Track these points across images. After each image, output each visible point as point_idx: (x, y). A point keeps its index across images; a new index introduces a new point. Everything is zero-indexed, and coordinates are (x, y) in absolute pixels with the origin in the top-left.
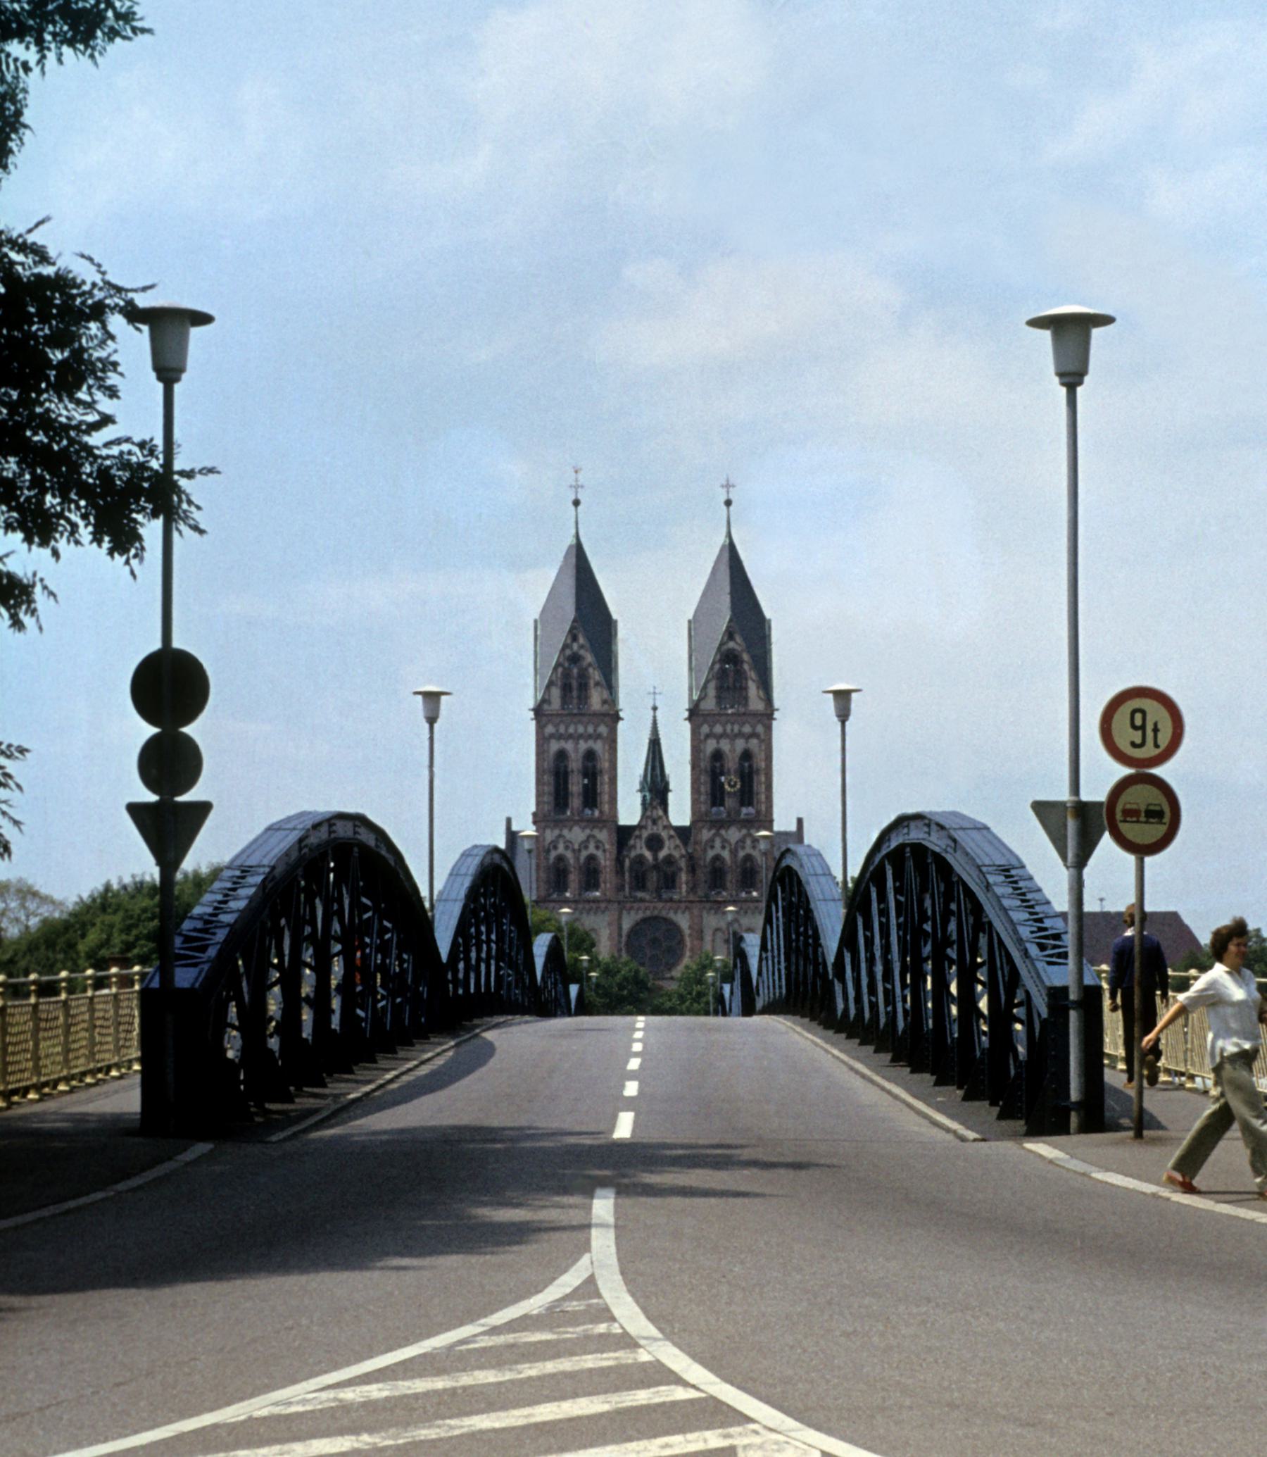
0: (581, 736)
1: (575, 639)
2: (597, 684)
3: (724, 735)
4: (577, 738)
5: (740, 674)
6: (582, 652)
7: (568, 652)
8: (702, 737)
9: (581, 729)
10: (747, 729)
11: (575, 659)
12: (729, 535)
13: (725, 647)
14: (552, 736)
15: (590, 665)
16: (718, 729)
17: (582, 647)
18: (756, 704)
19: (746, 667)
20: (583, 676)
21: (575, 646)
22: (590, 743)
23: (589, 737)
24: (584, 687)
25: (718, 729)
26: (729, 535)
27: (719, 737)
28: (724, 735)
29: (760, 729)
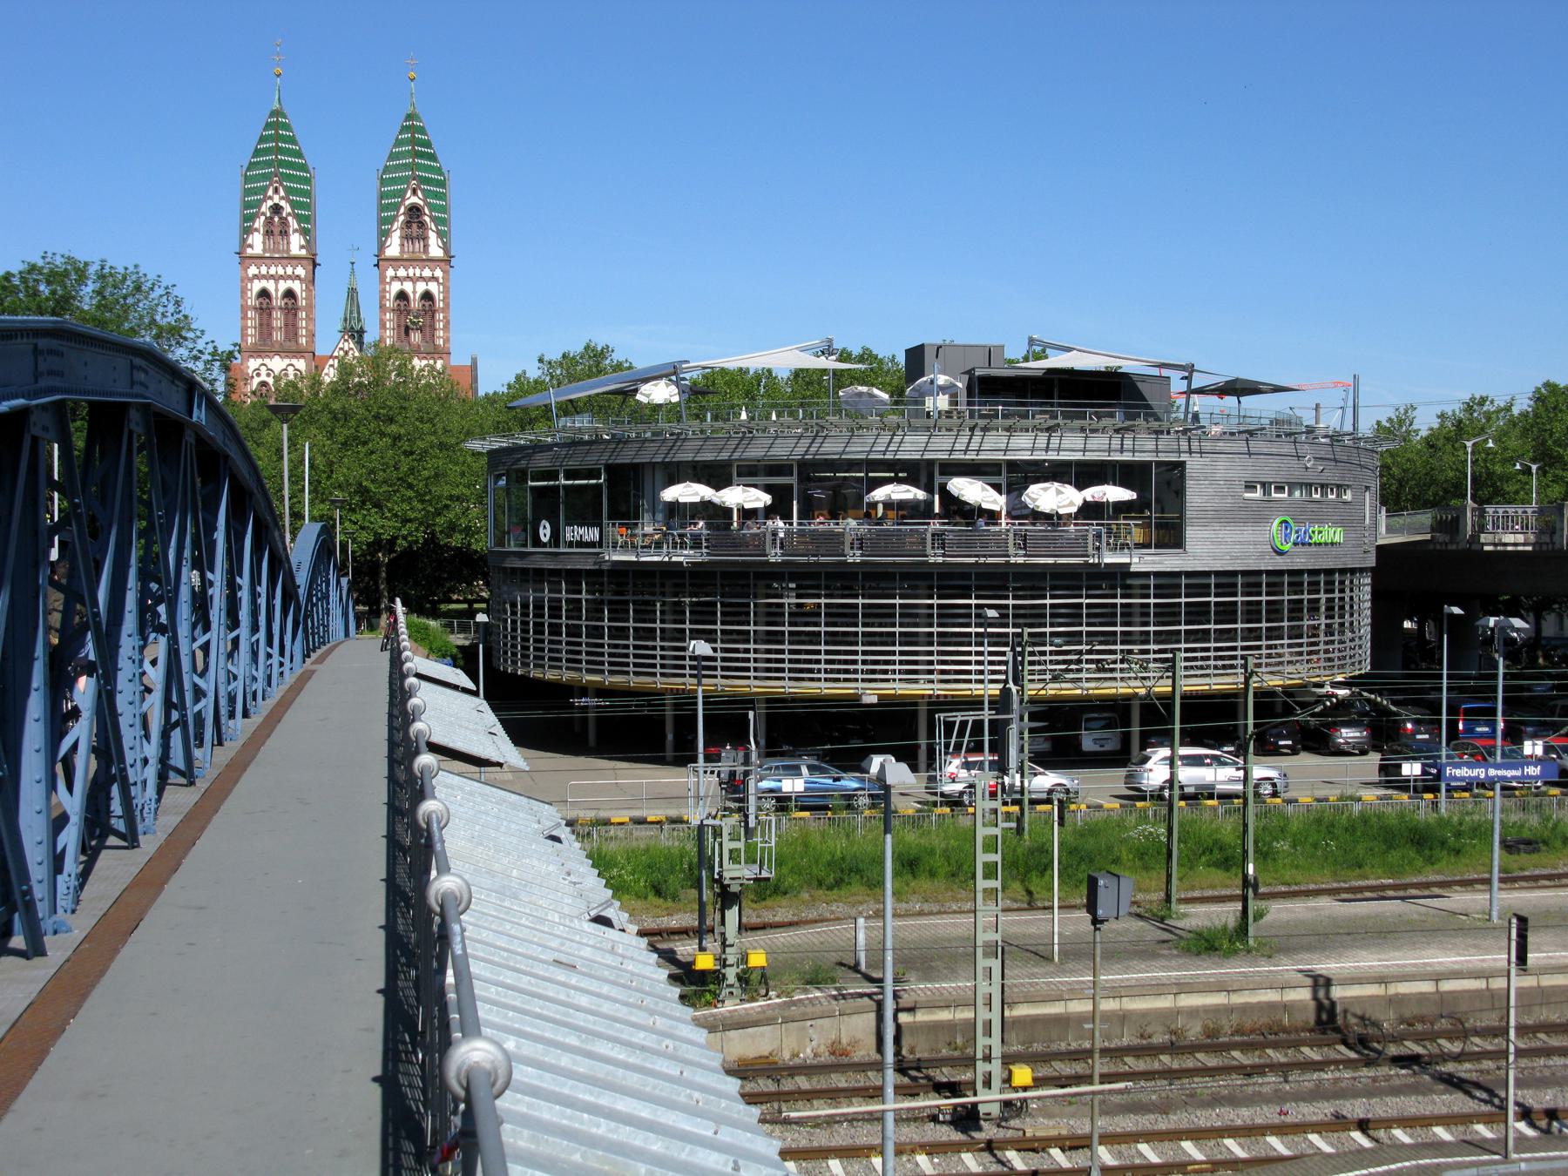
0: (281, 277)
1: (276, 191)
5: (422, 225)
6: (283, 203)
7: (270, 203)
9: (281, 271)
10: (427, 273)
11: (277, 209)
13: (407, 203)
14: (256, 277)
15: (289, 214)
17: (282, 198)
18: (436, 251)
19: (427, 219)
20: (284, 222)
22: (289, 284)
23: (285, 277)
24: (284, 233)
25: (402, 272)
29: (438, 273)
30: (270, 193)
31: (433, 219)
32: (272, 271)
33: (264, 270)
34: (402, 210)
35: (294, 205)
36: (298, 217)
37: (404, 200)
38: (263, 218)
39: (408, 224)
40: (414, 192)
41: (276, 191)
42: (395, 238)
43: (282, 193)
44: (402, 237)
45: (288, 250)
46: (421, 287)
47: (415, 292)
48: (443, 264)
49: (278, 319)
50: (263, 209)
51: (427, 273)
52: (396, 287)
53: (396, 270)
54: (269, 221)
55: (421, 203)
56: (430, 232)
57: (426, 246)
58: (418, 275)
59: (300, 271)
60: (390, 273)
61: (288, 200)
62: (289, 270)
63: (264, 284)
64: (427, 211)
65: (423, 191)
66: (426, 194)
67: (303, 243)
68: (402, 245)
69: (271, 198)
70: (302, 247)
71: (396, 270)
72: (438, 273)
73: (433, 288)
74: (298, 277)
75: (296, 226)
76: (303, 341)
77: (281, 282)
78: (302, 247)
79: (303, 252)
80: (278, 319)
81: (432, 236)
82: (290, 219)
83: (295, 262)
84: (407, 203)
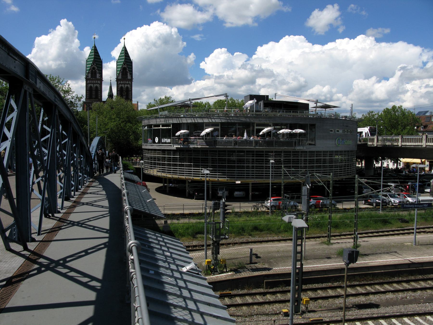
2: (98, 73)
3: (123, 84)
4: (94, 84)
6: (95, 67)
7: (92, 67)
9: (95, 82)
10: (127, 82)
11: (94, 68)
14: (89, 83)
16: (122, 82)
17: (95, 66)
18: (129, 77)
19: (127, 70)
21: (94, 66)
22: (97, 85)
23: (96, 83)
25: (122, 82)
27: (122, 84)
28: (123, 84)
31: (129, 70)
32: (93, 82)
33: (91, 82)
35: (98, 67)
36: (98, 70)
43: (95, 64)
44: (122, 75)
45: (96, 77)
46: (126, 85)
49: (94, 93)
51: (127, 82)
52: (120, 85)
53: (120, 82)
55: (126, 67)
57: (127, 77)
59: (99, 82)
61: (96, 66)
62: (97, 82)
63: (91, 85)
66: (127, 65)
68: (122, 76)
69: (93, 66)
71: (120, 82)
72: (130, 83)
74: (98, 83)
76: (100, 98)
78: (99, 77)
79: (100, 78)
80: (94, 93)
81: (129, 74)
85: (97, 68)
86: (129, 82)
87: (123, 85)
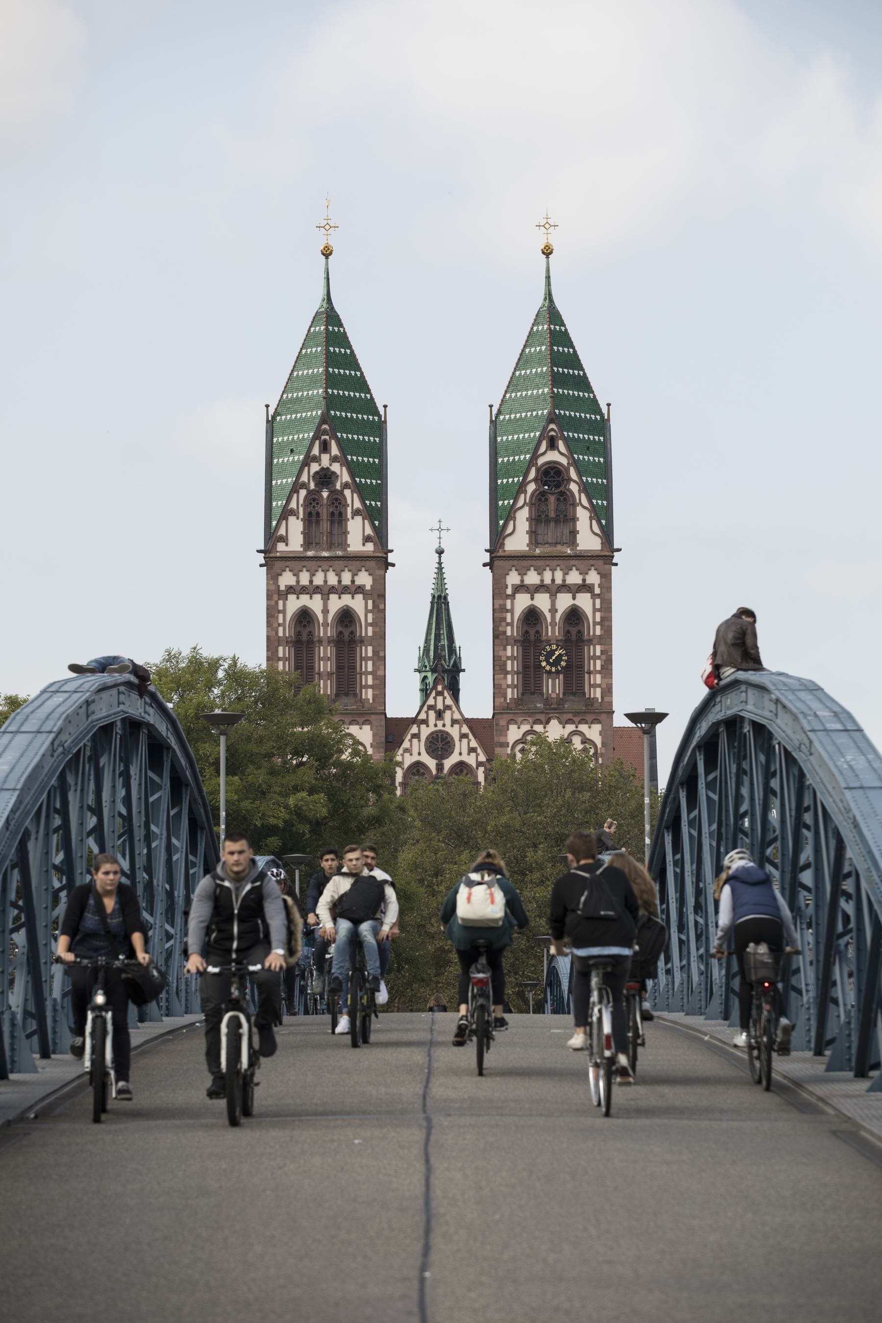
1: (325, 448)
2: (356, 513)
5: (566, 499)
6: (336, 468)
7: (315, 467)
8: (509, 591)
9: (333, 580)
10: (574, 578)
11: (325, 478)
12: (549, 296)
13: (541, 461)
15: (346, 486)
16: (532, 578)
17: (334, 459)
19: (574, 487)
20: (337, 499)
21: (325, 459)
22: (346, 600)
24: (338, 518)
25: (532, 578)
26: (549, 296)
29: (593, 578)
30: (316, 451)
34: (532, 474)
37: (535, 456)
38: (303, 493)
39: (539, 499)
40: (552, 445)
41: (325, 448)
42: (522, 517)
43: (335, 450)
46: (564, 601)
47: (553, 610)
48: (600, 563)
50: (304, 478)
51: (574, 578)
52: (522, 602)
54: (312, 499)
55: (564, 461)
56: (579, 509)
57: (574, 533)
58: (559, 581)
60: (513, 578)
64: (573, 474)
65: (566, 441)
67: (369, 531)
69: (316, 459)
70: (367, 539)
71: (522, 574)
73: (584, 602)
74: (360, 589)
75: (357, 504)
77: (333, 597)
78: (367, 539)
81: (583, 515)
82: (347, 493)
83: (357, 563)
84: (541, 461)
85: (346, 477)
86: (584, 573)
87: (542, 602)
